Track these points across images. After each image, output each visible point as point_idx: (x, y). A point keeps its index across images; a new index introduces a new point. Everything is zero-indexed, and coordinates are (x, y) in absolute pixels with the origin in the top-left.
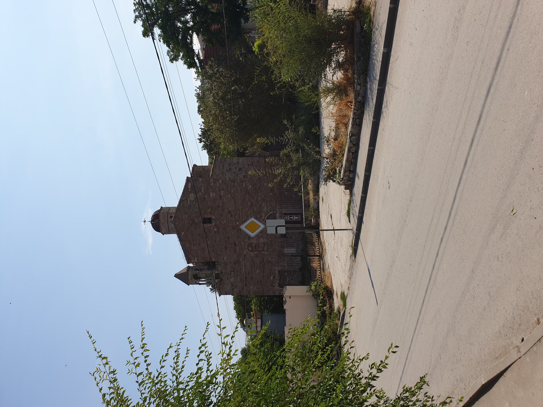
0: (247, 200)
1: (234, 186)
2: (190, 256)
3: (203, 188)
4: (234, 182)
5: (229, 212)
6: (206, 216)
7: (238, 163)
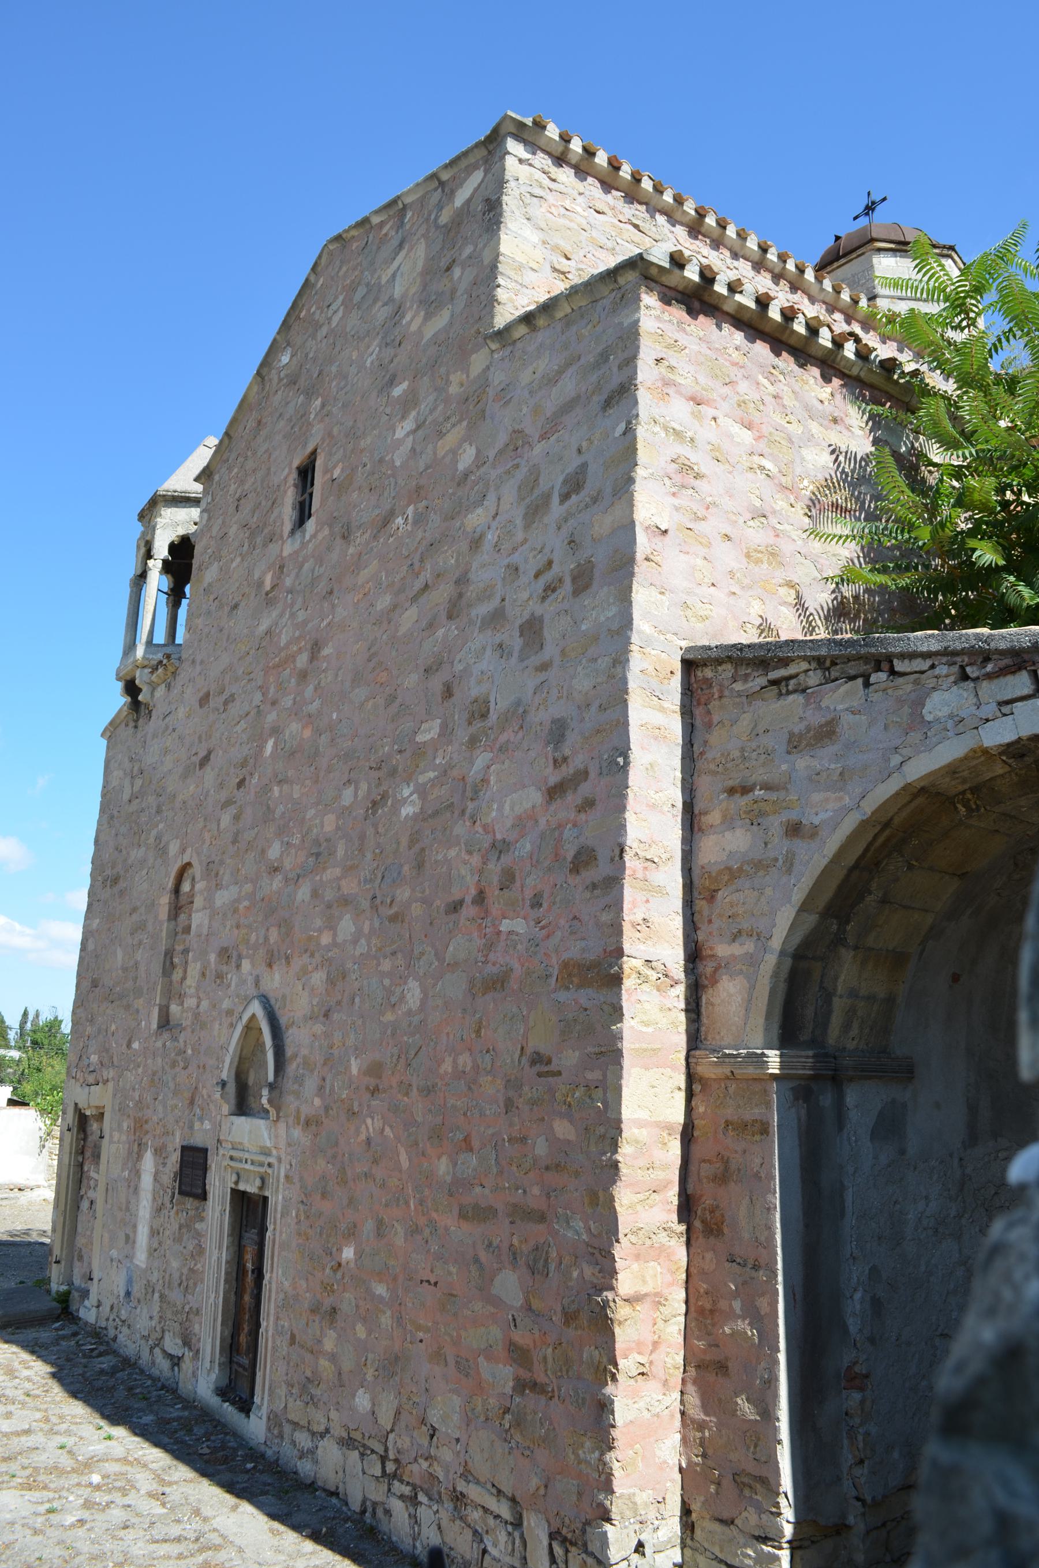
0: (348, 796)
1: (431, 626)
2: (216, 477)
3: (441, 320)
6: (318, 463)
7: (582, 580)
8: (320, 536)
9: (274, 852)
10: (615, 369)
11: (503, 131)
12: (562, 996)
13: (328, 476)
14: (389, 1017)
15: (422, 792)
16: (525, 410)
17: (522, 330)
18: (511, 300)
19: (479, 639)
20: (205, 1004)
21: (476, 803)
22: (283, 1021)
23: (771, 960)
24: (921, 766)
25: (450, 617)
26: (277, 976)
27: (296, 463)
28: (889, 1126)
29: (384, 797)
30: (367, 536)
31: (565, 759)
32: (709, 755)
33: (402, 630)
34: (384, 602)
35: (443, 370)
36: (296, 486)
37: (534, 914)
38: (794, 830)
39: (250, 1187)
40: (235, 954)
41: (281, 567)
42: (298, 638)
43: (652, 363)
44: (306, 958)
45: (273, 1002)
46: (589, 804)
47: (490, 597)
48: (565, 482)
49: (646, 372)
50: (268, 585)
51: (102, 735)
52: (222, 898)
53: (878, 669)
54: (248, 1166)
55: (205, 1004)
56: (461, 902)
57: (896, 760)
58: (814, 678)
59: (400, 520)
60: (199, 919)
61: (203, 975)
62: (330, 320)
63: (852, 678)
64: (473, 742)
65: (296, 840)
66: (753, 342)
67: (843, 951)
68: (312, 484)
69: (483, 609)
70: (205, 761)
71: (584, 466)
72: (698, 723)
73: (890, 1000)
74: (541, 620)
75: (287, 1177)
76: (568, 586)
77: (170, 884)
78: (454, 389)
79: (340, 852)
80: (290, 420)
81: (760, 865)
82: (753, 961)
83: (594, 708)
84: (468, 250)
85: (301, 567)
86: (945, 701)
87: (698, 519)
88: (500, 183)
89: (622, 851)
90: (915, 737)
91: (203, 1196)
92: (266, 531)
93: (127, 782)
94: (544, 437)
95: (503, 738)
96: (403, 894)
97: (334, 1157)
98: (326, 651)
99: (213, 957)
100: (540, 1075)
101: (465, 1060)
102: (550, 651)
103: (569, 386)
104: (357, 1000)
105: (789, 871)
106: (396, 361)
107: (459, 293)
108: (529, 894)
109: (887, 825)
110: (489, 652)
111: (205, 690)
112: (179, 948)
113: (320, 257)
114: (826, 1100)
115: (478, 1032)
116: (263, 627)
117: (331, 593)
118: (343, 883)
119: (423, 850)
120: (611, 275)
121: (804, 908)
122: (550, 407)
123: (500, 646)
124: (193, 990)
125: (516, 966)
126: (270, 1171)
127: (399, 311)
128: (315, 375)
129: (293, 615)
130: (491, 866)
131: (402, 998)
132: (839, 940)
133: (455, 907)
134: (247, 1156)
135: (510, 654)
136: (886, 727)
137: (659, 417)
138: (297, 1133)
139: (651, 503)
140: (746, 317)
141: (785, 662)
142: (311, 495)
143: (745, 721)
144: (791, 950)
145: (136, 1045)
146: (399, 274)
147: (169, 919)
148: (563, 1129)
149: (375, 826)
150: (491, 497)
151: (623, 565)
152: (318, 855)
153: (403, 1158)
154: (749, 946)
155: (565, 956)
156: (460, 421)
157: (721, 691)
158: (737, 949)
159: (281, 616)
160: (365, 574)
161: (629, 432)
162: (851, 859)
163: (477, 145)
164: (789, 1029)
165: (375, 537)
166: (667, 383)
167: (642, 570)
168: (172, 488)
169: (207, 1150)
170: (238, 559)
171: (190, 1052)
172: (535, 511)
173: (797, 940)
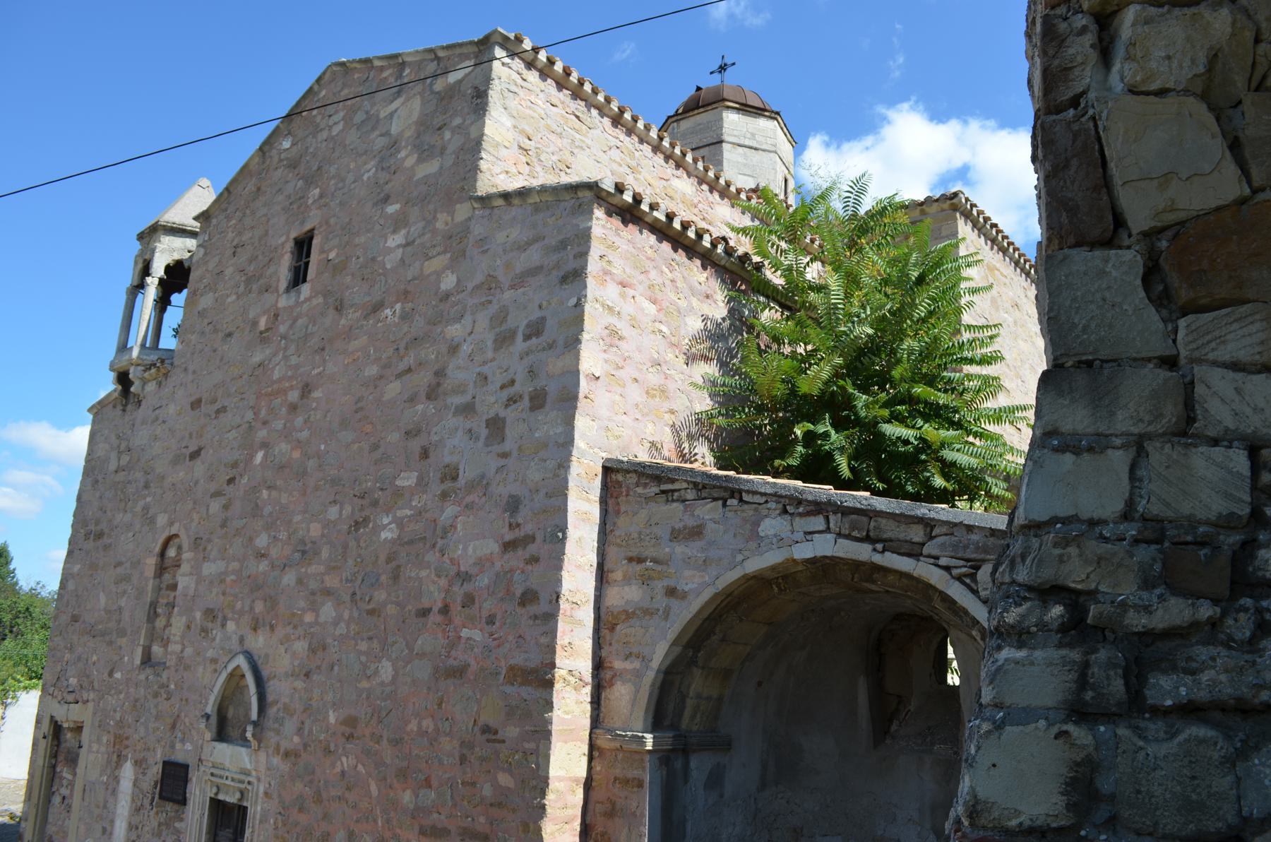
0: (333, 512)
1: (412, 400)
2: (214, 221)
3: (432, 167)
4: (432, 394)
5: (306, 390)
6: (315, 242)
7: (538, 401)
8: (315, 302)
9: (262, 541)
10: (571, 257)
11: (493, 39)
12: (508, 689)
13: (324, 256)
14: (364, 684)
15: (400, 523)
16: (499, 262)
17: (500, 202)
18: (489, 169)
19: (451, 421)
20: (189, 651)
21: (445, 541)
22: (265, 673)
23: (650, 676)
24: (755, 564)
25: (429, 397)
26: (261, 639)
27: (294, 235)
28: (715, 780)
29: (366, 520)
30: (358, 314)
31: (518, 525)
32: (617, 533)
33: (386, 397)
34: (372, 371)
35: (431, 207)
36: (292, 253)
37: (489, 628)
38: (671, 592)
39: (231, 798)
40: (220, 615)
41: (276, 316)
42: (291, 378)
43: (597, 258)
44: (289, 629)
45: (256, 658)
46: (534, 560)
47: (463, 392)
48: (528, 326)
49: (593, 265)
50: (262, 324)
51: (90, 410)
52: (209, 569)
53: (732, 497)
54: (228, 782)
55: (189, 651)
56: (429, 610)
57: (740, 558)
58: (690, 495)
59: (388, 312)
60: (184, 581)
61: (189, 627)
62: (331, 127)
63: (715, 499)
64: (444, 495)
65: (283, 535)
66: (661, 242)
67: (695, 669)
68: (308, 255)
69: (458, 400)
70: (195, 455)
71: (543, 319)
72: (610, 509)
73: (720, 699)
74: (504, 420)
75: (266, 794)
76: (526, 402)
77: (158, 549)
78: (439, 225)
79: (325, 553)
80: (289, 197)
81: (648, 612)
82: (638, 674)
83: (542, 494)
84: (458, 121)
85: (295, 321)
86: (772, 525)
87: (618, 368)
88: (488, 79)
89: (558, 597)
90: (752, 545)
91: (183, 802)
92: (262, 281)
93: (113, 455)
94: (512, 287)
95: (469, 499)
96: (380, 596)
97: (311, 782)
98: (317, 394)
99: (198, 615)
100: (488, 741)
101: (428, 724)
102: (508, 445)
103: (534, 256)
104: (336, 668)
105: (666, 618)
106: (390, 185)
107: (448, 152)
108: (485, 614)
109: (730, 595)
110: (460, 433)
111: (197, 396)
112: (163, 601)
113: (324, 73)
114: (678, 764)
115: (440, 705)
116: (257, 359)
117: (323, 349)
118: (327, 578)
119: (399, 566)
120: (574, 188)
121: (674, 643)
122: (519, 267)
123: (470, 431)
124: (177, 638)
125: (473, 663)
126: (249, 787)
127: (394, 145)
128: (315, 168)
129: (286, 358)
130: (455, 589)
131: (376, 672)
132: (693, 662)
133: (424, 613)
134: (227, 774)
135: (477, 438)
136: (735, 536)
137: (600, 294)
138: (276, 760)
139: (591, 359)
140: (659, 226)
141: (673, 481)
142: (307, 264)
143: (643, 514)
144: (663, 668)
145: (118, 675)
146: (396, 116)
147: (155, 577)
148: (504, 779)
149: (357, 540)
150: (468, 320)
151: (569, 400)
152: (304, 552)
153: (374, 789)
154: (634, 664)
155: (512, 662)
156: (444, 252)
157: (628, 491)
158: (628, 665)
159: (275, 355)
160: (355, 344)
161: (579, 305)
162: (706, 614)
163: (471, 43)
164: (658, 720)
165: (366, 317)
166: (606, 273)
167: (582, 404)
168: (171, 220)
169: (187, 766)
170: (234, 297)
171: (172, 686)
172: (504, 339)
173: (668, 662)
